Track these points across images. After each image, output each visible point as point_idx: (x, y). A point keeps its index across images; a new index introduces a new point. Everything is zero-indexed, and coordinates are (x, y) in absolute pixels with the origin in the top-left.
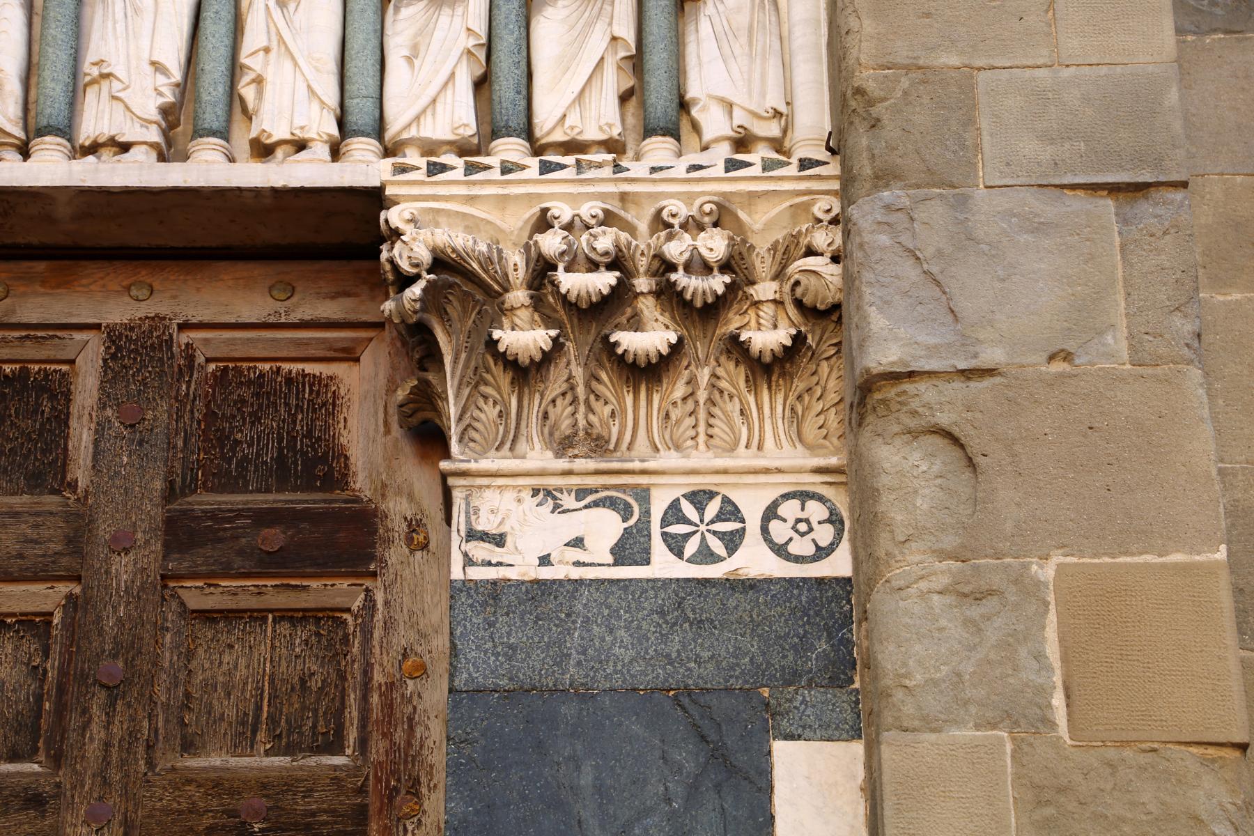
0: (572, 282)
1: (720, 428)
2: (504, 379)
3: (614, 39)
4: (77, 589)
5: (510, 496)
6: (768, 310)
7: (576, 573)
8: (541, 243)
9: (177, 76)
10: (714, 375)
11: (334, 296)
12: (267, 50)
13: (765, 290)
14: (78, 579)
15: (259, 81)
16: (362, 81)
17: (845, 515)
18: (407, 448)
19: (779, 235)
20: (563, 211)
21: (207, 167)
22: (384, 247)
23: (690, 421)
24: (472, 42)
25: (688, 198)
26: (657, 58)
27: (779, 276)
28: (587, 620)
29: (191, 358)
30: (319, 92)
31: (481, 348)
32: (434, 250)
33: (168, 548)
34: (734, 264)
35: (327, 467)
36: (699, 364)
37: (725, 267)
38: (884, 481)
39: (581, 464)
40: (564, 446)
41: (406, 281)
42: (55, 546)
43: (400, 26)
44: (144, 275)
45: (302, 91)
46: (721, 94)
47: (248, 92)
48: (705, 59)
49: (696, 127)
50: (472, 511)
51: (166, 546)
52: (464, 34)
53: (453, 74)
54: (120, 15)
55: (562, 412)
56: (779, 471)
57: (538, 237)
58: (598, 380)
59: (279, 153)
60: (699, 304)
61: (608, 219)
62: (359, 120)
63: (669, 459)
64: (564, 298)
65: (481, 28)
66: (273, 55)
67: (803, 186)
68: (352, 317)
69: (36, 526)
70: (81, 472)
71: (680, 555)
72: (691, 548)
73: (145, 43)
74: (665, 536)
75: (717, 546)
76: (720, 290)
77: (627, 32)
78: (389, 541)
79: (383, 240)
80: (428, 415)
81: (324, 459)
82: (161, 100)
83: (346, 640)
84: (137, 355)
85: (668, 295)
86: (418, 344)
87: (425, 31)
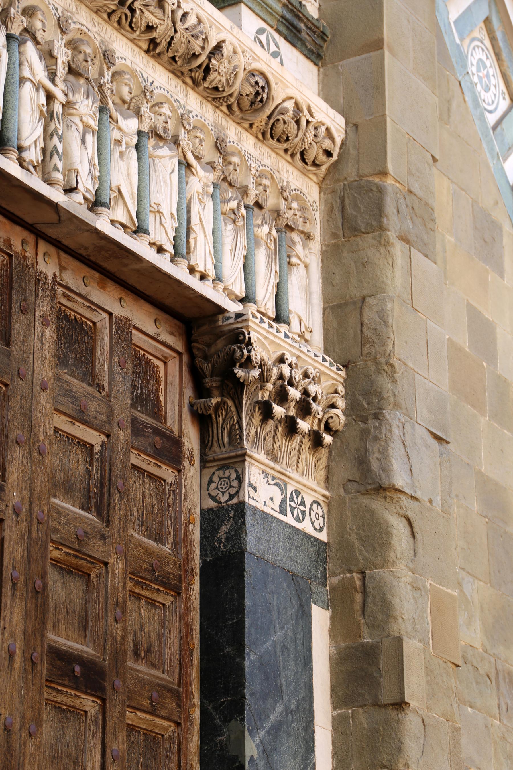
8: (283, 369)
11: (171, 334)
38: (394, 531)
51: (132, 431)
56: (316, 491)
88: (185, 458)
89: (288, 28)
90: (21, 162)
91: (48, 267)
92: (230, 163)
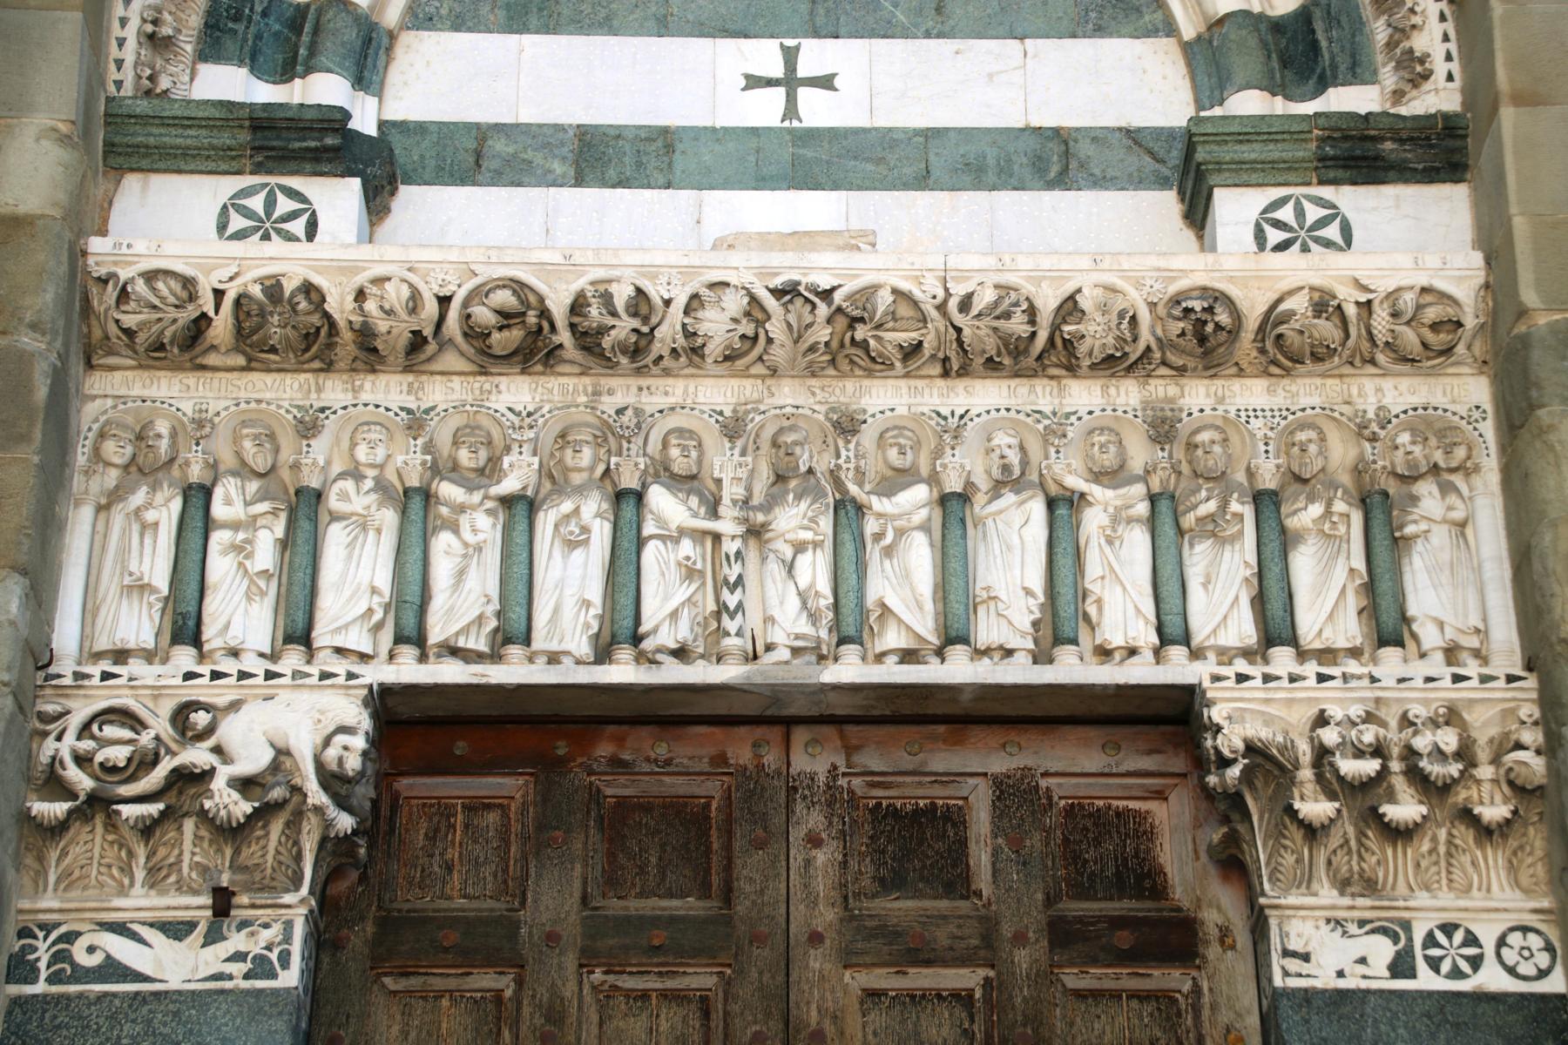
0: (1350, 767)
1: (1457, 875)
2: (1298, 835)
3: (1352, 570)
4: (992, 973)
5: (1310, 924)
6: (1486, 788)
7: (1364, 984)
9: (1042, 599)
10: (1450, 834)
11: (1150, 752)
12: (1103, 578)
13: (1485, 772)
14: (993, 967)
15: (1099, 601)
16: (1171, 603)
17: (1557, 945)
18: (1213, 871)
19: (1494, 731)
20: (1335, 712)
21: (1071, 668)
22: (1208, 735)
23: (1434, 869)
24: (1248, 573)
25: (1426, 702)
26: (1384, 586)
27: (1496, 761)
28: (1375, 1020)
29: (1050, 798)
30: (1144, 610)
31: (1279, 810)
32: (1245, 740)
33: (1053, 945)
34: (1465, 754)
35: (1149, 881)
36: (1439, 826)
37: (1459, 755)
39: (1360, 901)
40: (1343, 885)
41: (1225, 763)
42: (974, 942)
43: (1195, 559)
44: (1013, 736)
45: (1131, 611)
46: (1434, 614)
47: (1092, 610)
48: (1419, 586)
49: (1414, 636)
50: (1284, 935)
51: (1050, 942)
52: (1242, 566)
53: (1237, 598)
54: (997, 552)
55: (1340, 859)
56: (1506, 910)
57: (1320, 731)
58: (1366, 836)
59: (1117, 656)
60: (1440, 784)
61: (1369, 718)
62: (1172, 632)
63: (1422, 899)
64: (1341, 779)
65: (1252, 558)
66: (1107, 580)
67: (1509, 695)
68: (1163, 769)
69: (959, 927)
70: (983, 880)
71: (1437, 971)
72: (1446, 967)
73: (1018, 572)
74: (1426, 958)
75: (1464, 966)
76: (1456, 775)
77: (1359, 563)
78: (1207, 942)
79: (1206, 729)
80: (1234, 851)
81: (1149, 875)
82: (1032, 617)
83: (1179, 1014)
84: (1015, 796)
85: (1416, 776)
86: (1231, 806)
87: (1215, 562)
88: (1207, 942)
89: (1345, 167)
90: (643, 658)
91: (801, 762)
92: (1196, 446)
